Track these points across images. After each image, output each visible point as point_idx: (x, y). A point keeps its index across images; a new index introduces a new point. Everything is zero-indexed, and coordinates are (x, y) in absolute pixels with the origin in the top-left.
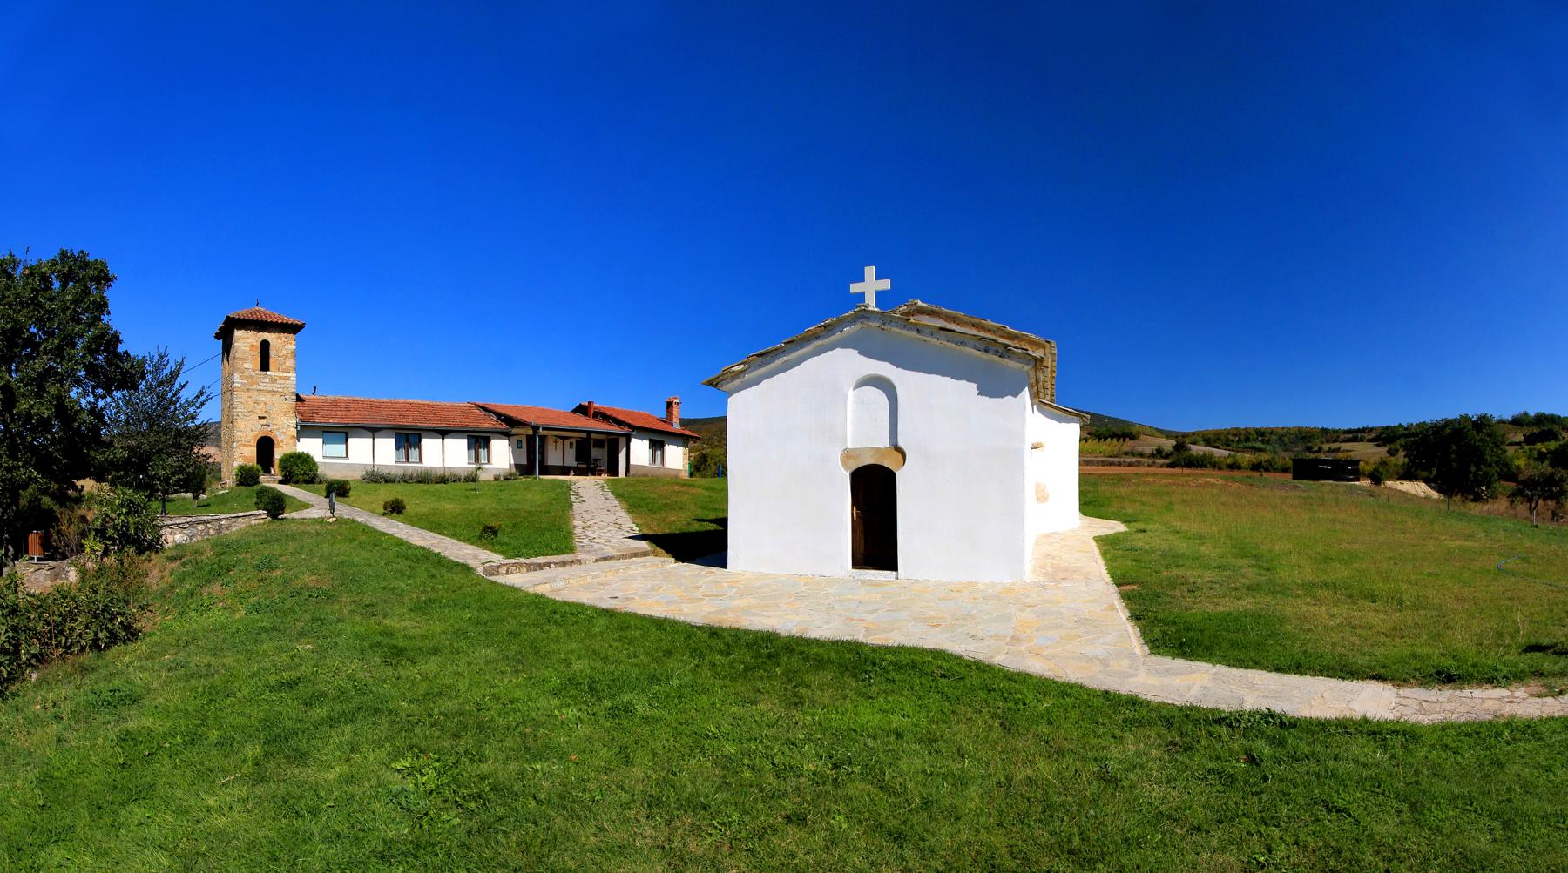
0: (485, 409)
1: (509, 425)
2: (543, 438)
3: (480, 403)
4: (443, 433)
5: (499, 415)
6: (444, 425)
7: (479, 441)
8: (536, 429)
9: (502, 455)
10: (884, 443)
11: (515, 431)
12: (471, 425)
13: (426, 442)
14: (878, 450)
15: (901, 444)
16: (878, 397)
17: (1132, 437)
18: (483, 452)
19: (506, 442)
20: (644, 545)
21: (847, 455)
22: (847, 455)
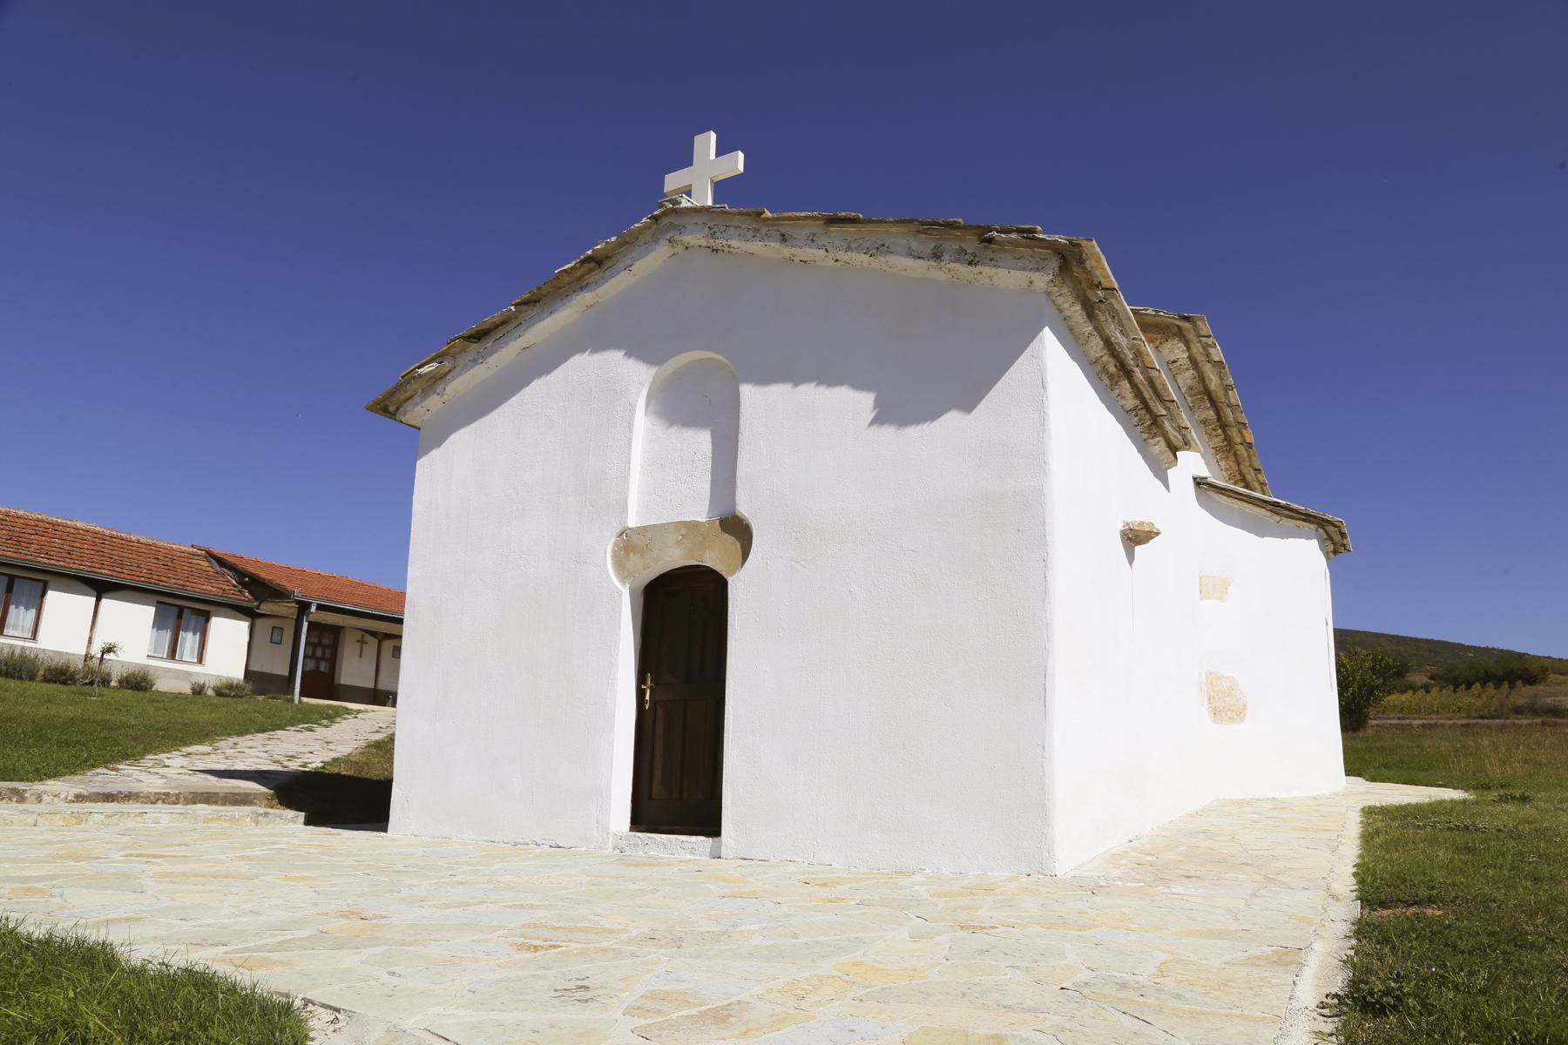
0: (221, 562)
1: (254, 594)
2: (336, 631)
3: (218, 550)
4: (101, 588)
6: (105, 573)
7: (182, 612)
8: (304, 607)
9: (227, 647)
11: (266, 608)
12: (170, 583)
13: (54, 598)
14: (692, 526)
17: (1530, 679)
18: (189, 640)
21: (630, 544)
22: (630, 544)
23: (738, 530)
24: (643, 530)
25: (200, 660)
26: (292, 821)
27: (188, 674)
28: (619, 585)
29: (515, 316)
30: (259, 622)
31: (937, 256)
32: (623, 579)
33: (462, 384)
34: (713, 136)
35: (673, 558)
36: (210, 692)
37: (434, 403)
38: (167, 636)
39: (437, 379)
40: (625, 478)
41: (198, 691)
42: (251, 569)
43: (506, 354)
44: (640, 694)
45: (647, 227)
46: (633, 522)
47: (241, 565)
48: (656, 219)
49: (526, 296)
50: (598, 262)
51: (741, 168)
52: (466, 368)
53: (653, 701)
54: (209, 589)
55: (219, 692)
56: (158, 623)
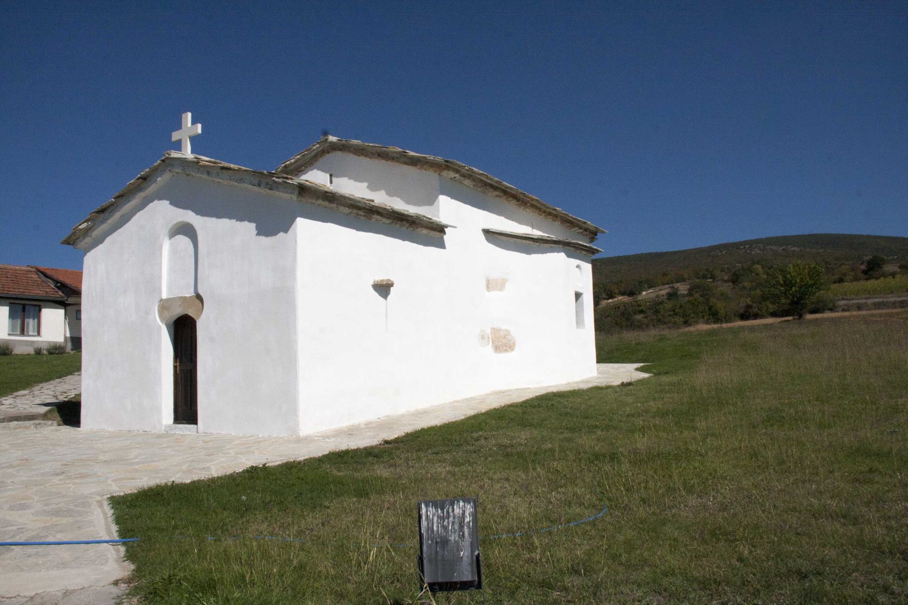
3: (42, 267)
5: (56, 282)
10: (190, 293)
12: (15, 291)
14: (184, 299)
15: (201, 292)
16: (183, 241)
18: (31, 323)
19: (61, 312)
20: (44, 409)
21: (164, 306)
22: (164, 306)
23: (199, 297)
24: (168, 300)
25: (39, 334)
26: (52, 425)
27: (33, 342)
28: (160, 323)
29: (112, 204)
30: (69, 308)
31: (259, 185)
32: (162, 321)
33: (96, 233)
34: (189, 115)
35: (178, 311)
36: (45, 352)
37: (88, 240)
38: (19, 322)
39: (88, 230)
40: (160, 277)
41: (38, 352)
42: (61, 278)
43: (117, 215)
44: (175, 367)
45: (159, 165)
46: (165, 296)
47: (55, 276)
48: (163, 161)
49: (118, 194)
50: (144, 178)
51: (200, 131)
52: (99, 226)
53: (181, 370)
54: (39, 292)
55: (50, 353)
56: (12, 315)
